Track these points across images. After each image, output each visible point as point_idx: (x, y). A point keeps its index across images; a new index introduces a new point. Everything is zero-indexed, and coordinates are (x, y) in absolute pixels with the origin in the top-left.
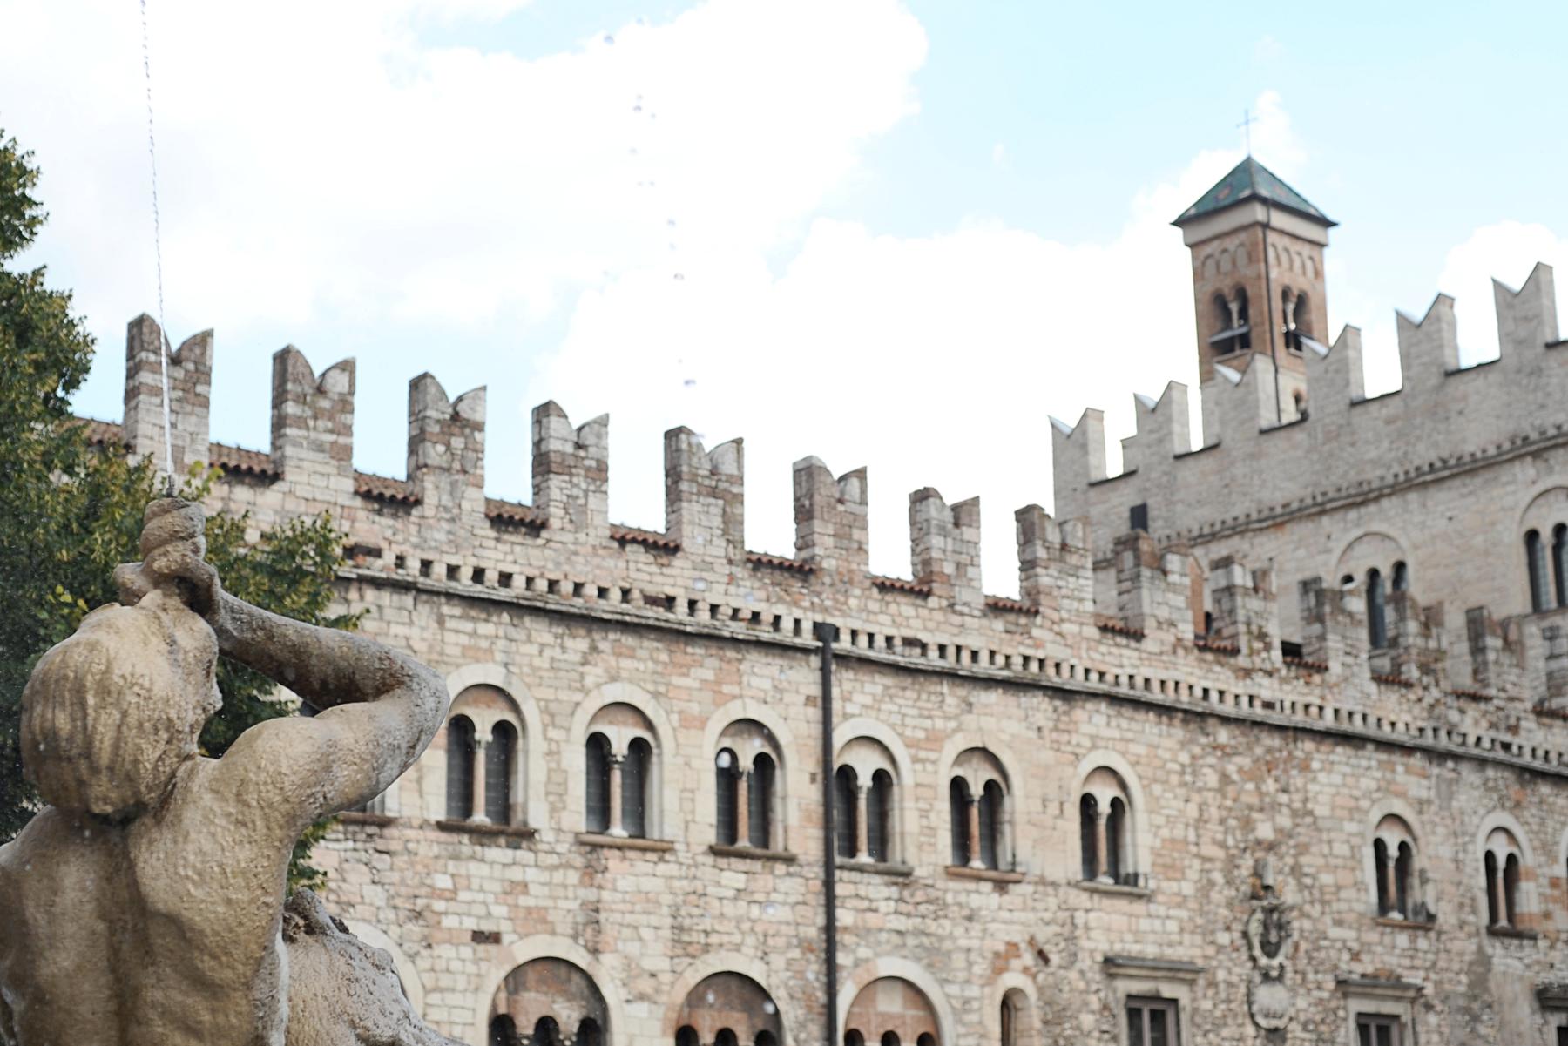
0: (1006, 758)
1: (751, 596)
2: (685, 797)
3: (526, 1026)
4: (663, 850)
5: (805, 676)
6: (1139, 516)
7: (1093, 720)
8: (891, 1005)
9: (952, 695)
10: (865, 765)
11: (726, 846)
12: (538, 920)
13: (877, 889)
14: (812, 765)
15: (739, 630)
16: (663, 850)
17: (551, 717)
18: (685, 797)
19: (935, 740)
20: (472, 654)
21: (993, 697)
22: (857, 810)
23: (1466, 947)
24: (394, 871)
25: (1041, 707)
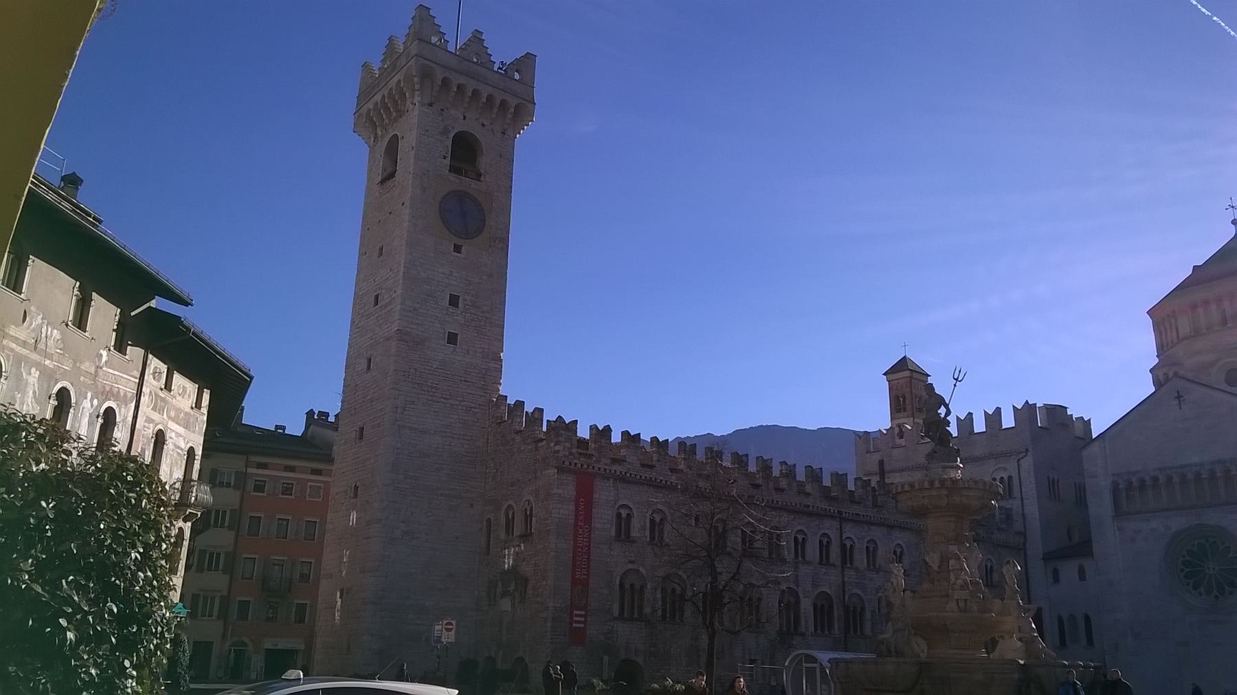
1: (824, 505)
2: (812, 551)
4: (809, 563)
5: (836, 524)
6: (881, 463)
10: (848, 543)
13: (852, 573)
16: (809, 563)
18: (812, 551)
22: (847, 554)
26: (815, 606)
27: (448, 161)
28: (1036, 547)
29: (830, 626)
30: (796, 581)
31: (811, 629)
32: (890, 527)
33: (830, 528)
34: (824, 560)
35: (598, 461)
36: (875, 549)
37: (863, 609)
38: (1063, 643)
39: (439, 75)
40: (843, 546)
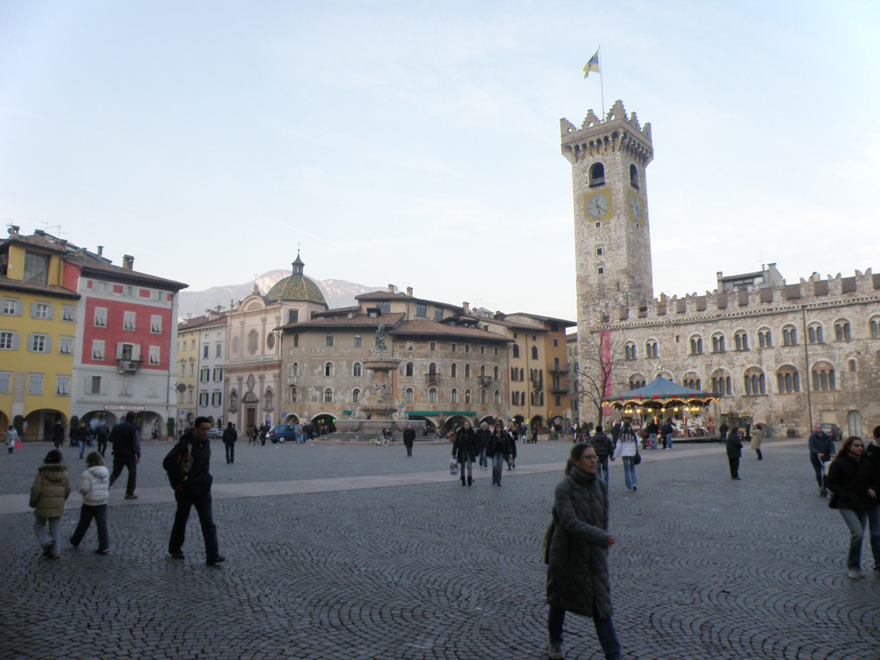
0: (849, 319)
2: (777, 338)
3: (751, 376)
4: (773, 348)
5: (800, 315)
8: (822, 366)
9: (833, 311)
11: (786, 345)
12: (751, 362)
13: (818, 347)
14: (802, 329)
15: (785, 311)
16: (773, 348)
17: (751, 332)
19: (830, 319)
20: (737, 326)
21: (844, 309)
22: (814, 335)
24: (728, 358)
25: (858, 308)
26: (779, 376)
27: (588, 184)
29: (797, 389)
30: (760, 361)
32: (866, 304)
33: (795, 320)
35: (613, 322)
36: (847, 326)
37: (832, 371)
39: (573, 146)
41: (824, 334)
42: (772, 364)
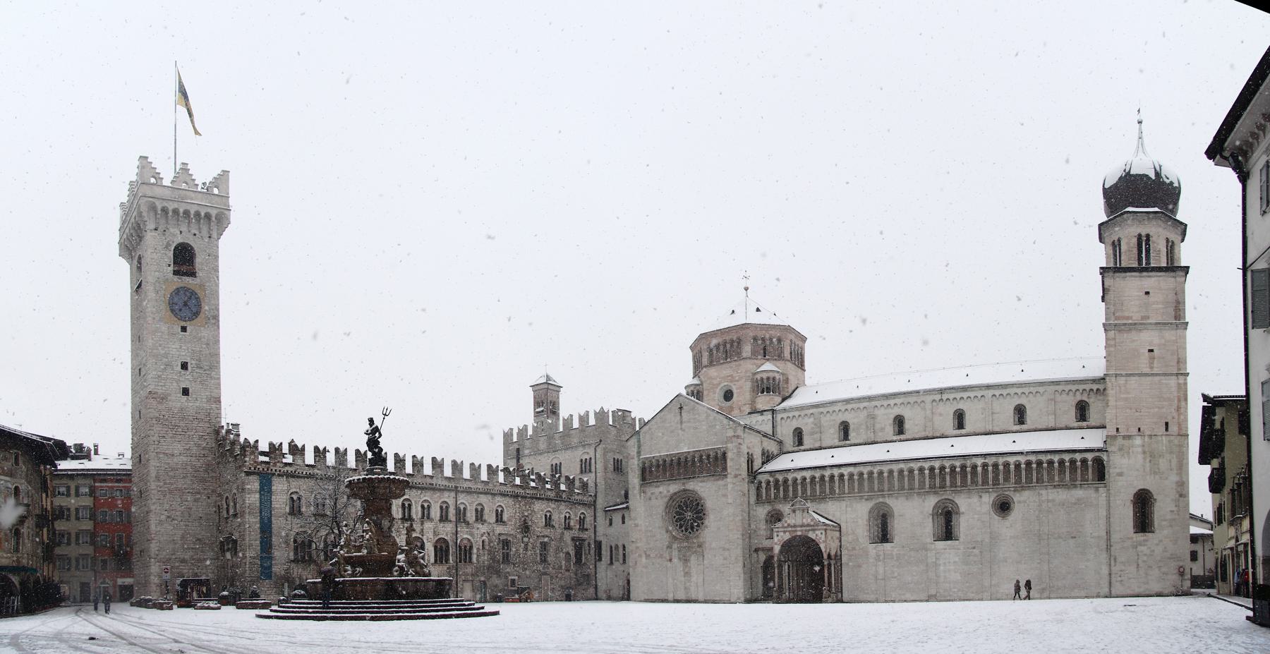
1: (445, 483)
2: (435, 513)
5: (453, 494)
7: (498, 498)
10: (462, 507)
16: (432, 520)
18: (435, 513)
22: (461, 515)
23: (559, 531)
25: (490, 497)
26: (435, 547)
28: (601, 503)
29: (447, 561)
31: (432, 560)
33: (449, 498)
34: (444, 518)
36: (482, 510)
37: (471, 547)
38: (611, 563)
40: (457, 509)
41: (468, 514)
42: (431, 535)
